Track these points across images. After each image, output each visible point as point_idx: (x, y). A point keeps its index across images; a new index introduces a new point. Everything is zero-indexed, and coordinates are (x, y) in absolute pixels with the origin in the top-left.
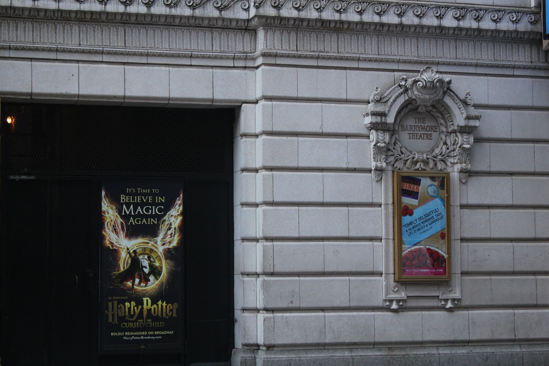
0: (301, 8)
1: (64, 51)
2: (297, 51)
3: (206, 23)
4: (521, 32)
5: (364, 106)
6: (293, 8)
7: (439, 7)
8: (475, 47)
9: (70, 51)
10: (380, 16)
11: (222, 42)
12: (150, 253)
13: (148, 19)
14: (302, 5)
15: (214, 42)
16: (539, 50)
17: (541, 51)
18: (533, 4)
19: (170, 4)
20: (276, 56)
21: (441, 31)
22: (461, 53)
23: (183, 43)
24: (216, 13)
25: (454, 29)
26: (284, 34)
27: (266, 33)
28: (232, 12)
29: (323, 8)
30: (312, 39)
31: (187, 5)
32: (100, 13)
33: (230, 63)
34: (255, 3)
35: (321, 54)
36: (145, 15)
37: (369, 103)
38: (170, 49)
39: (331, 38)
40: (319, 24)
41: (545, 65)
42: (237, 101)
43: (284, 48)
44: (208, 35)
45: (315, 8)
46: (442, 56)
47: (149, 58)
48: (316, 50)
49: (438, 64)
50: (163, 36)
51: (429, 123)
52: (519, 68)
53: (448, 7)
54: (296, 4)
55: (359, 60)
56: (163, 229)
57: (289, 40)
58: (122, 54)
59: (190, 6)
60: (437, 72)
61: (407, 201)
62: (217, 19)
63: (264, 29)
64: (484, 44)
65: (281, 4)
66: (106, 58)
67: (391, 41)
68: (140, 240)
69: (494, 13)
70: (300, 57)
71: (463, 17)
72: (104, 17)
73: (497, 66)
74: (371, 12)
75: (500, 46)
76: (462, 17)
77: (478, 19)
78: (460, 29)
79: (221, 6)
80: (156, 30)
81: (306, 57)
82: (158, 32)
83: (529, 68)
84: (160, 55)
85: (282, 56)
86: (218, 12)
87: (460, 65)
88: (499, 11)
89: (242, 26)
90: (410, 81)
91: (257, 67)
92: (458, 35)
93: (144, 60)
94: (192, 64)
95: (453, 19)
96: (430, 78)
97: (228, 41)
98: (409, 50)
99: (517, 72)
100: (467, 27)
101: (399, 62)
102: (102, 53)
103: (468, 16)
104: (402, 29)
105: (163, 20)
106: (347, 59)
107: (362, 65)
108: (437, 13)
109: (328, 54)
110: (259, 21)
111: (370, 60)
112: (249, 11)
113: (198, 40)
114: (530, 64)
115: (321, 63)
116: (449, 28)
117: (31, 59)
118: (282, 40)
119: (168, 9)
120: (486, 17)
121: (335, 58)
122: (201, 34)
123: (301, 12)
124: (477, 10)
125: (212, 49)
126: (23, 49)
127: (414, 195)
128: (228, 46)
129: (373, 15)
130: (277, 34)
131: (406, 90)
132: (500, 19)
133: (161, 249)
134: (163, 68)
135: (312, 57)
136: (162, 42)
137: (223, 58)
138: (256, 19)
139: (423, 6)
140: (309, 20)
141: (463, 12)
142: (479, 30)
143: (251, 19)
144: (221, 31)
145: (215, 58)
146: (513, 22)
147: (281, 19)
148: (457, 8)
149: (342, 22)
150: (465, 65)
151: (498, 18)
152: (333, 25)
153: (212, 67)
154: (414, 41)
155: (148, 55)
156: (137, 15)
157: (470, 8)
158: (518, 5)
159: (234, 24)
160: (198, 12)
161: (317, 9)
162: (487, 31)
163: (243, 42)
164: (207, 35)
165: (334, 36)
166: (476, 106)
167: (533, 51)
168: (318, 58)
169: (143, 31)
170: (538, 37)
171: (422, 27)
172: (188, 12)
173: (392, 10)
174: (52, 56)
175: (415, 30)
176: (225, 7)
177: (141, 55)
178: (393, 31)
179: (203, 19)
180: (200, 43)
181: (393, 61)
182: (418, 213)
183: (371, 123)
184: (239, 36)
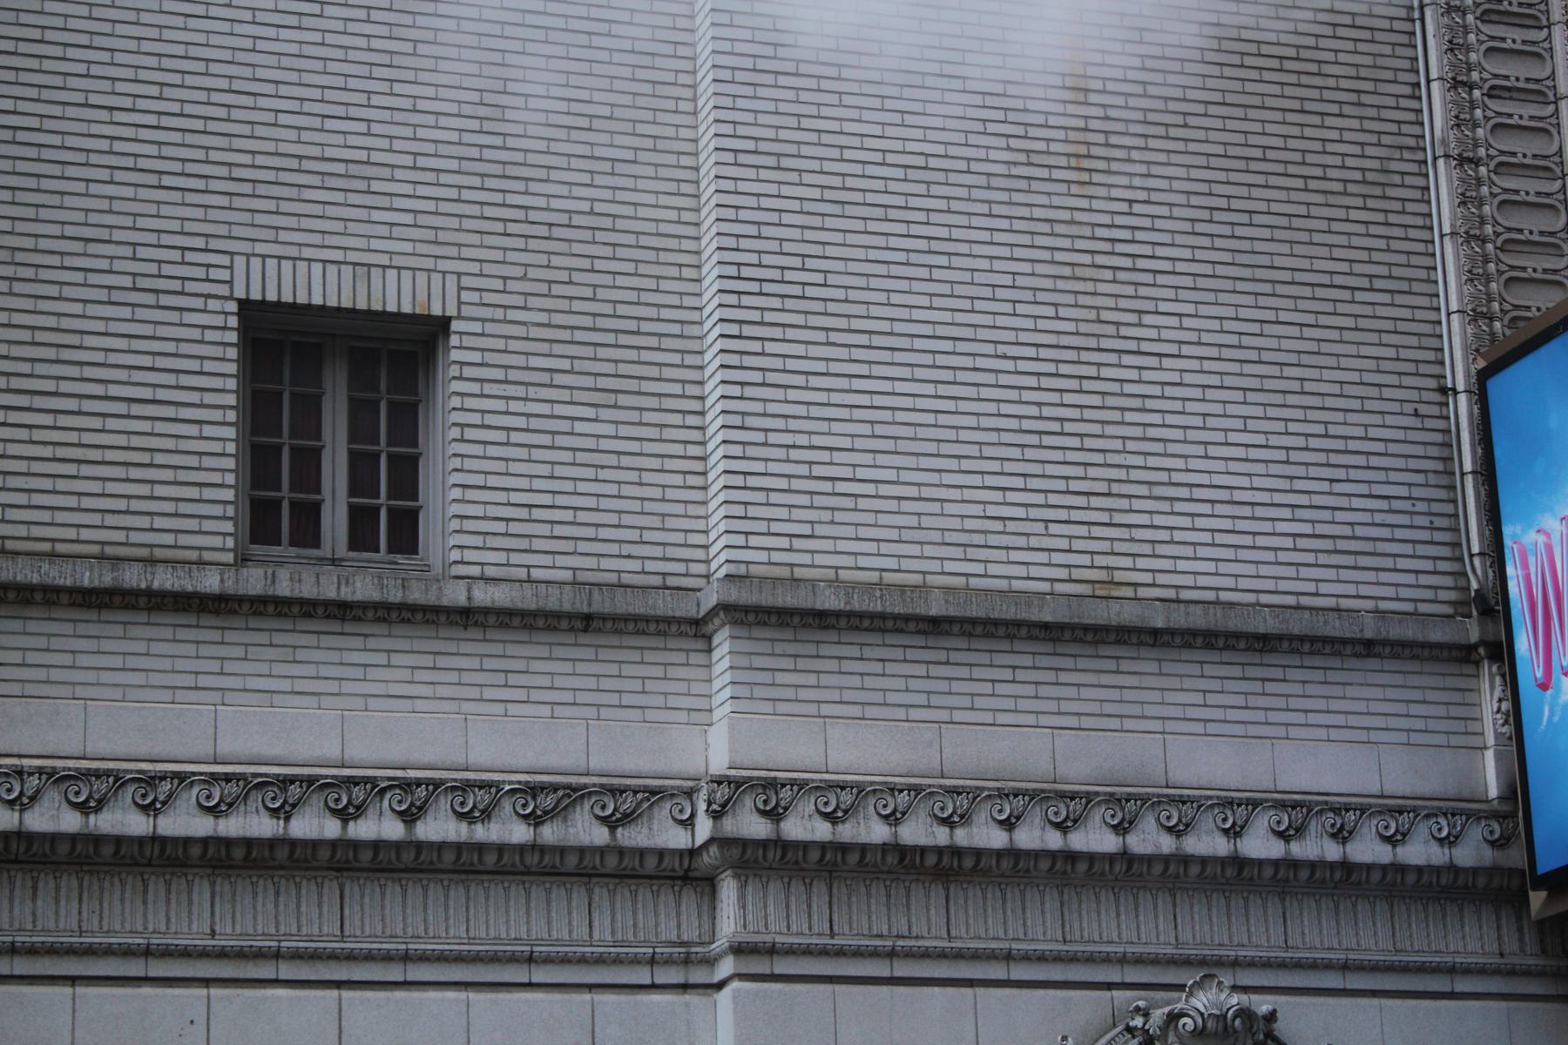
0: (840, 814)
1: (167, 953)
2: (832, 935)
3: (572, 861)
4: (1466, 870)
6: (816, 816)
7: (1230, 803)
8: (1337, 915)
9: (186, 953)
10: (1065, 833)
11: (619, 916)
13: (408, 857)
14: (843, 806)
15: (596, 915)
16: (1519, 919)
17: (1525, 923)
18: (1493, 792)
19: (471, 811)
20: (772, 951)
21: (1240, 872)
22: (1298, 931)
23: (507, 922)
24: (600, 835)
25: (1276, 863)
26: (793, 890)
27: (742, 888)
28: (645, 831)
29: (904, 814)
30: (873, 901)
31: (517, 813)
32: (272, 843)
33: (642, 976)
34: (709, 804)
35: (900, 943)
36: (398, 846)
38: (471, 940)
39: (928, 897)
40: (892, 859)
41: (1541, 962)
43: (794, 928)
44: (579, 897)
45: (878, 814)
46: (1246, 941)
47: (410, 966)
48: (885, 932)
49: (1235, 964)
50: (451, 903)
52: (1467, 971)
53: (1255, 804)
54: (826, 804)
55: (1009, 957)
57: (809, 907)
58: (333, 956)
59: (525, 817)
60: (1235, 988)
62: (602, 851)
63: (737, 876)
64: (1363, 907)
65: (783, 803)
66: (287, 971)
67: (1098, 902)
69: (1387, 817)
70: (840, 953)
71: (965, 818)
72: (282, 854)
73: (1405, 969)
74: (1037, 821)
75: (1408, 909)
76: (1297, 830)
77: (1341, 835)
78: (1293, 864)
79: (613, 814)
80: (432, 885)
81: (858, 953)
82: (436, 892)
83: (1496, 972)
84: (442, 958)
85: (790, 951)
86: (606, 830)
87: (1298, 965)
88: (1401, 813)
89: (673, 870)
90: (1158, 1015)
91: (720, 986)
92: (1287, 881)
93: (395, 973)
94: (534, 980)
95: (1270, 835)
96: (1214, 1005)
97: (635, 913)
98: (1152, 926)
99: (1462, 985)
100: (1311, 858)
101: (1123, 960)
102: (277, 955)
103: (1314, 826)
104: (1129, 868)
105: (449, 857)
106: (975, 956)
107: (1020, 972)
108: (1225, 820)
109: (920, 943)
110: (722, 854)
111: (1042, 958)
112: (693, 825)
113: (549, 911)
114: (1497, 960)
115: (903, 969)
116: (1260, 863)
118: (788, 906)
119: (464, 826)
120: (1365, 830)
121: (942, 955)
122: (558, 894)
123: (840, 827)
124: (1336, 810)
125: (591, 936)
126: (52, 951)
128: (635, 925)
129: (1043, 829)
130: (775, 887)
132: (1404, 835)
134: (451, 994)
135: (874, 954)
136: (447, 919)
137: (621, 962)
138: (714, 850)
139: (1184, 803)
140: (864, 848)
141: (1298, 815)
142: (1346, 866)
143: (700, 847)
144: (616, 885)
145: (600, 961)
146: (1441, 841)
147: (784, 846)
148: (1281, 805)
149: (956, 852)
150: (1314, 966)
151: (1290, 825)
152: (931, 860)
153: (591, 987)
154: (1163, 901)
155: (406, 958)
156: (377, 845)
157: (1318, 803)
158: (1452, 793)
159: (651, 863)
160: (550, 833)
161: (886, 817)
162: (1370, 867)
163: (678, 914)
164: (575, 896)
165: (937, 892)
167: (1504, 921)
168: (892, 954)
169: (393, 890)
170: (1516, 883)
171: (1185, 860)
172: (520, 833)
173: (1097, 816)
174: (134, 968)
175: (1166, 868)
176: (626, 816)
177: (387, 958)
178: (1103, 874)
179: (562, 850)
180: (556, 919)
181: (1107, 959)
184: (667, 897)
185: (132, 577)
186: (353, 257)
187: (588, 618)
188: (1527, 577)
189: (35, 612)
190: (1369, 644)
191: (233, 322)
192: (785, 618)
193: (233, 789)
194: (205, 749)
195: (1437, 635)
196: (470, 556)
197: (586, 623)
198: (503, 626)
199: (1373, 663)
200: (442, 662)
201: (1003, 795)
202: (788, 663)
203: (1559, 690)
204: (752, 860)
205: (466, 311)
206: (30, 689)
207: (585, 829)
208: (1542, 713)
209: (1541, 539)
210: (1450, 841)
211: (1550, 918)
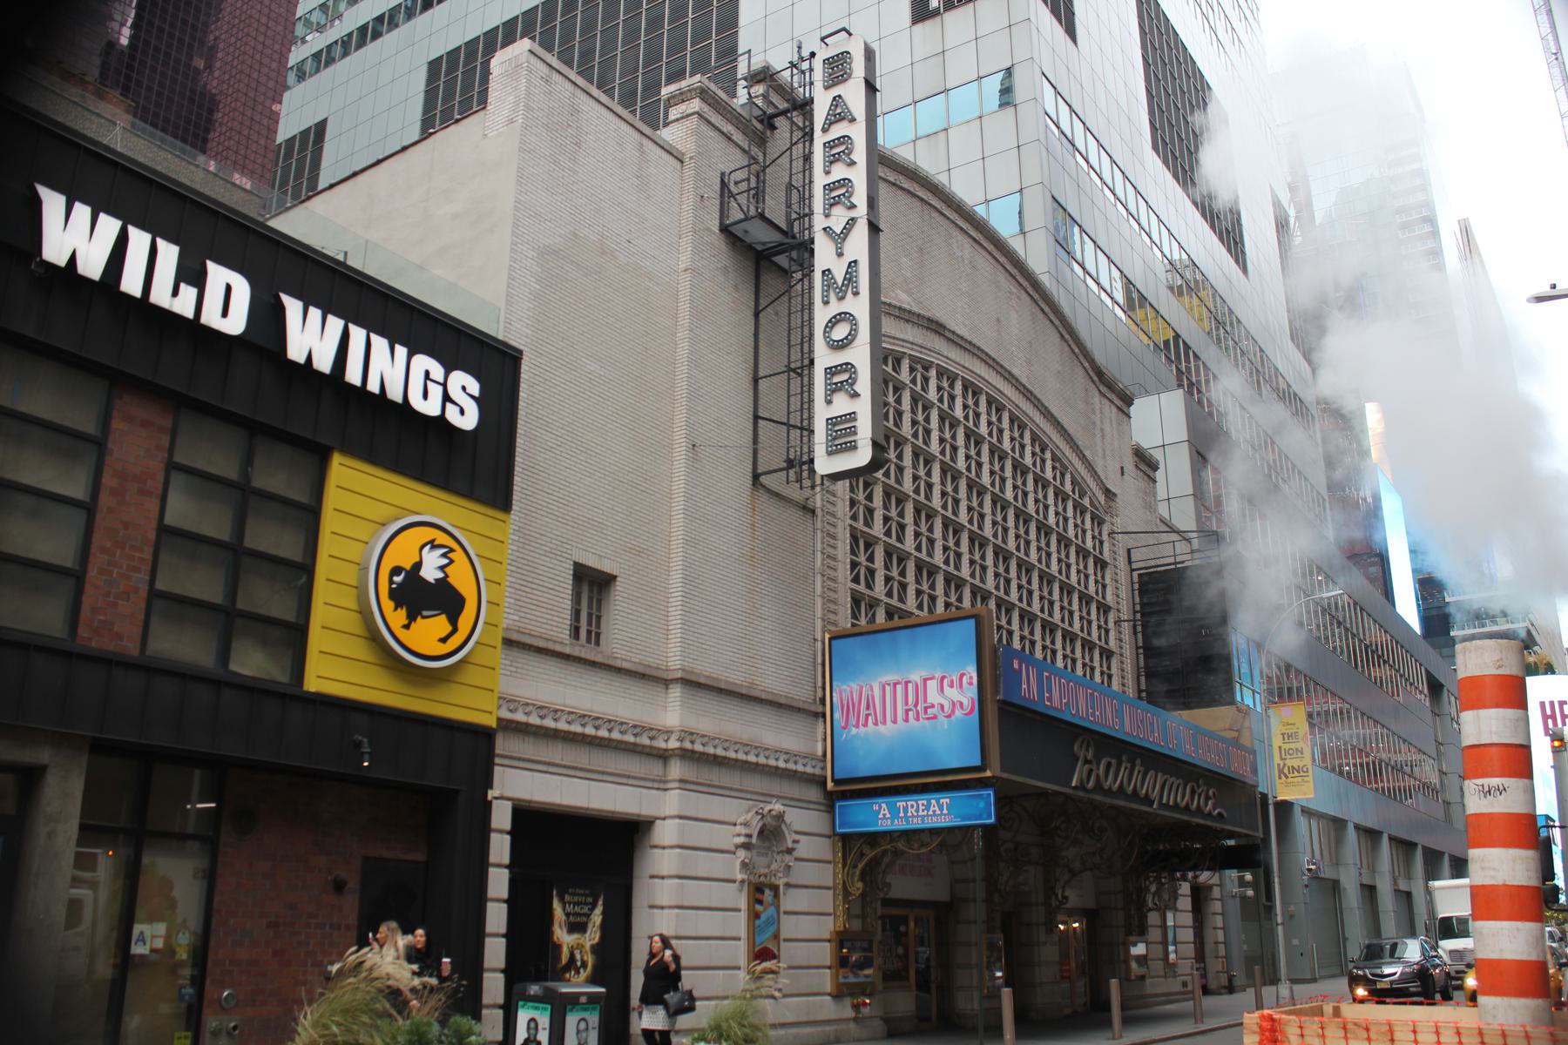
12: (581, 947)
33: (649, 784)
56: (590, 925)
61: (758, 907)
68: (576, 936)
127: (760, 902)
133: (588, 945)
182: (763, 917)
185: (551, 646)
192: (692, 684)
195: (813, 708)
197: (643, 676)
204: (687, 755)
207: (644, 740)
208: (842, 736)
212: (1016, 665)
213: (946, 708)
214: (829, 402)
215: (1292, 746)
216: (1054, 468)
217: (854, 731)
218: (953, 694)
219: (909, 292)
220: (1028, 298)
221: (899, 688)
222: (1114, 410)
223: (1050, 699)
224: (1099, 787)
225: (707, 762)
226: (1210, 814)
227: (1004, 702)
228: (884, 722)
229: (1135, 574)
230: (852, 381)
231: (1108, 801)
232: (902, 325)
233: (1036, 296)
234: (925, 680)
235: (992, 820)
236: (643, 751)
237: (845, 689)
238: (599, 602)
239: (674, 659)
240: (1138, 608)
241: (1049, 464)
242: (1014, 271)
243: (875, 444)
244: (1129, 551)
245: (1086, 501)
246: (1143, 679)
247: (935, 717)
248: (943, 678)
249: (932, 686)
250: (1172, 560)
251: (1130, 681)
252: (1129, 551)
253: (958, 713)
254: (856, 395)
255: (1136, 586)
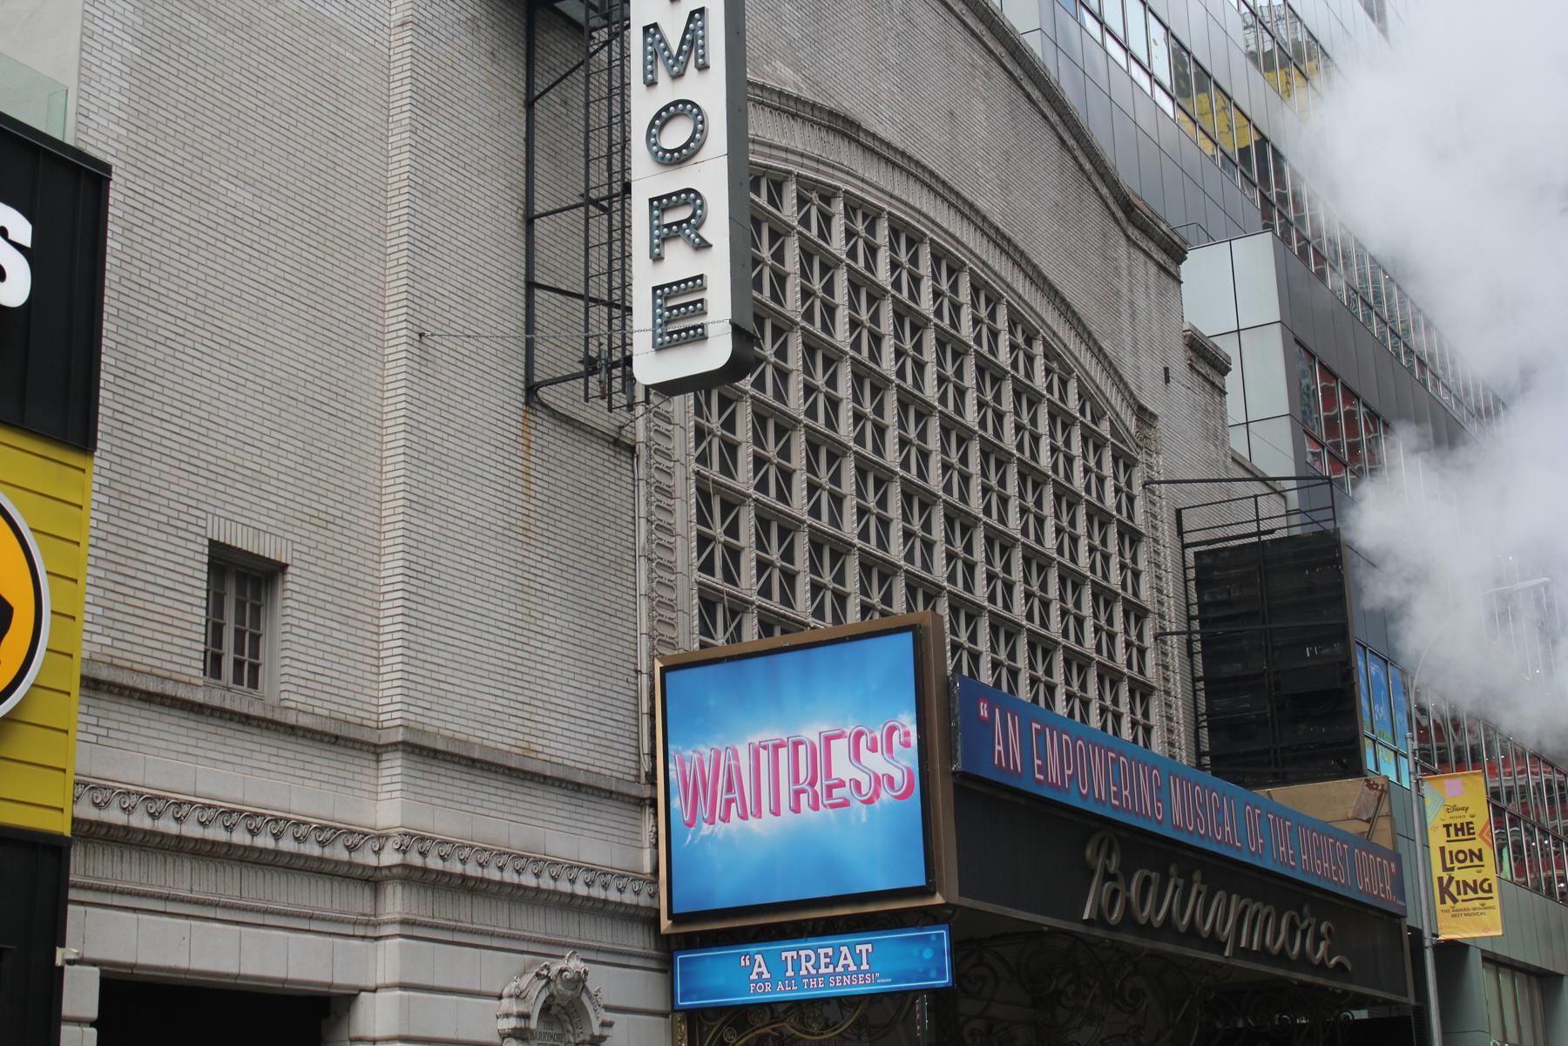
5: (496, 1002)
20: (413, 923)
33: (349, 930)
37: (500, 997)
40: (419, 874)
42: (355, 988)
51: (556, 1030)
60: (583, 960)
115: (458, 937)
117: (135, 910)
126: (130, 893)
131: (548, 984)
166: (608, 1008)
174: (160, 906)
183: (515, 1029)
185: (169, 689)
186: (254, 524)
187: (337, 737)
188: (684, 772)
189: (124, 701)
190: (611, 792)
191: (206, 551)
192: (423, 752)
193: (211, 812)
194: (190, 789)
195: (634, 792)
196: (293, 697)
197: (334, 740)
198: (304, 737)
199: (610, 802)
200: (282, 753)
201: (501, 854)
202: (420, 774)
203: (700, 828)
204: (414, 877)
205: (296, 563)
206: (122, 745)
207: (339, 852)
208: (685, 839)
209: (695, 756)
210: (637, 893)
211: (677, 935)
212: (984, 713)
213: (864, 789)
214: (657, 258)
215: (1465, 846)
216: (1048, 371)
217: (706, 829)
218: (875, 762)
219: (797, 67)
220: (1003, 76)
221: (783, 752)
222: (1153, 269)
223: (1043, 769)
224: (1129, 918)
225: (450, 889)
226: (1322, 964)
227: (964, 776)
228: (758, 814)
229: (1190, 552)
230: (697, 221)
231: (1147, 944)
232: (786, 123)
233: (1018, 72)
234: (828, 739)
235: (946, 980)
236: (336, 871)
237: (690, 756)
238: (256, 610)
239: (389, 710)
240: (1195, 611)
241: (1039, 364)
242: (979, 28)
243: (738, 331)
244: (1179, 512)
245: (1104, 428)
246: (1204, 733)
247: (846, 803)
248: (859, 735)
249: (840, 748)
250: (1253, 528)
251: (1182, 737)
252: (1179, 512)
253: (886, 795)
254: (703, 246)
255: (1192, 574)
